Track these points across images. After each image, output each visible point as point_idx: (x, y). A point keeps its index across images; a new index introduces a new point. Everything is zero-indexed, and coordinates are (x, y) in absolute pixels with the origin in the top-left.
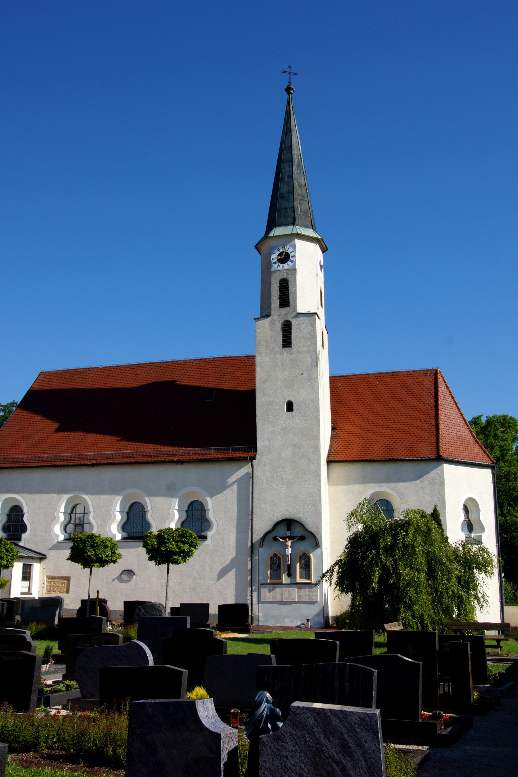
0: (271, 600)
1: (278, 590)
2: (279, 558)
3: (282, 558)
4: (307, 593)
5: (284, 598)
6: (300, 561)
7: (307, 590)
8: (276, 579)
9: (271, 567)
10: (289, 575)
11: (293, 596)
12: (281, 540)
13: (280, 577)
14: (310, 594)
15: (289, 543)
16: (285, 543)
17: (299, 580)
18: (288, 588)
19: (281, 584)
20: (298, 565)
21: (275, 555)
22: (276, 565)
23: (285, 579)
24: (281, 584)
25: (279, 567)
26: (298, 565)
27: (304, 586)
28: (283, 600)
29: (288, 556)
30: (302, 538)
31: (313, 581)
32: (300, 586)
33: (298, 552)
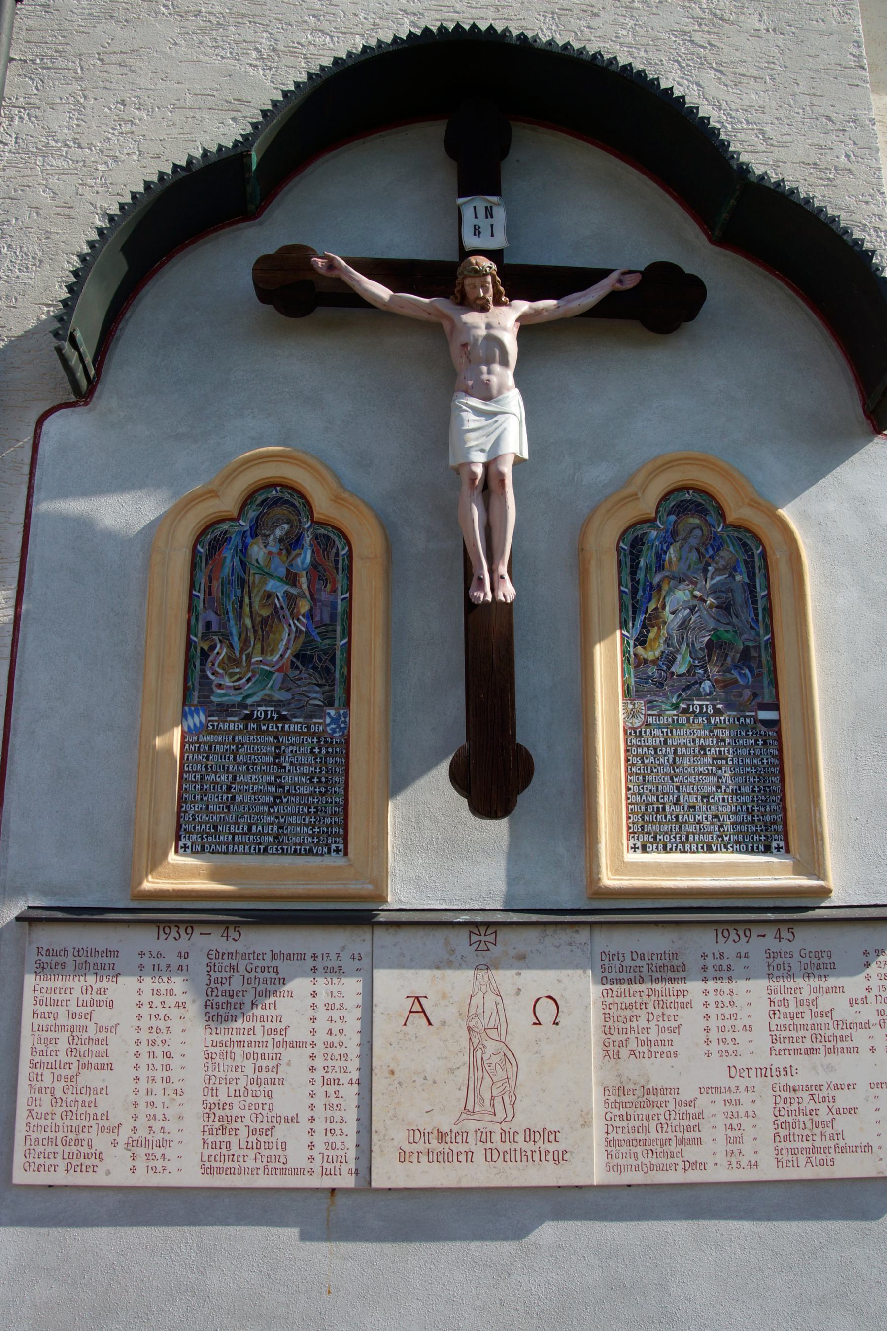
0: (185, 1170)
1: (309, 1001)
2: (332, 543)
3: (366, 543)
4: (756, 1048)
5: (389, 1136)
6: (637, 605)
7: (753, 994)
8: (279, 844)
9: (195, 659)
10: (493, 775)
11: (530, 1113)
12: (382, 292)
13: (331, 824)
14: (807, 1071)
15: (506, 320)
16: (438, 331)
17: (625, 865)
18: (461, 980)
19: (358, 915)
20: (608, 660)
21: (275, 503)
22: (284, 644)
23: (430, 846)
24: (358, 915)
25: (322, 664)
26: (608, 660)
27: (702, 942)
28: (388, 1173)
29: (489, 487)
30: (660, 304)
31: (845, 882)
32: (657, 942)
33: (600, 474)
